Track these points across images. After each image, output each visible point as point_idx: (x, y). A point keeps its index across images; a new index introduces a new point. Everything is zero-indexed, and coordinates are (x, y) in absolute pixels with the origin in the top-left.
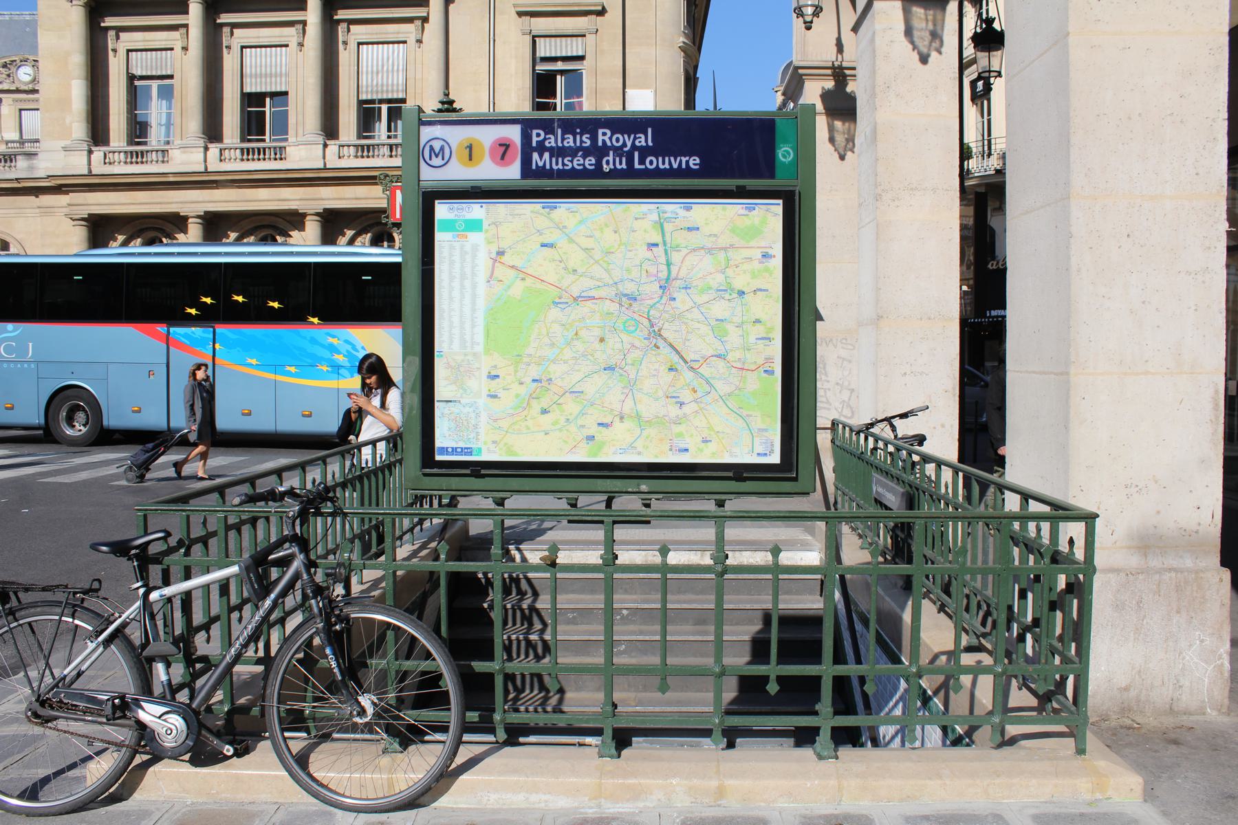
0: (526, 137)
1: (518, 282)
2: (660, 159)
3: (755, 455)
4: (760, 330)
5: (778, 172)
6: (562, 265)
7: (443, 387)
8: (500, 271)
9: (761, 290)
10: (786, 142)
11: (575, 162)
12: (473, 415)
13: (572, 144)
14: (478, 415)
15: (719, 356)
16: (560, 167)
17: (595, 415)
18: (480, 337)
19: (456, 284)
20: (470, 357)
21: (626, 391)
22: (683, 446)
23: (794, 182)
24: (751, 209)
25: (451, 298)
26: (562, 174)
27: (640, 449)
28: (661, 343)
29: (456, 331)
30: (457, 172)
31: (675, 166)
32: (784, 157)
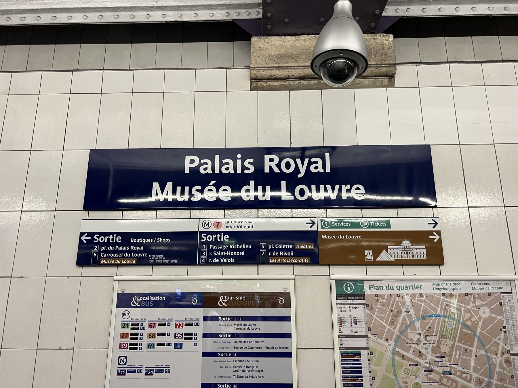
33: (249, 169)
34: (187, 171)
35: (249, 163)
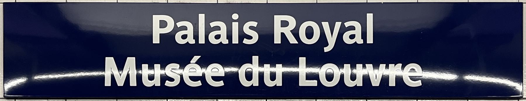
33: (250, 38)
34: (156, 40)
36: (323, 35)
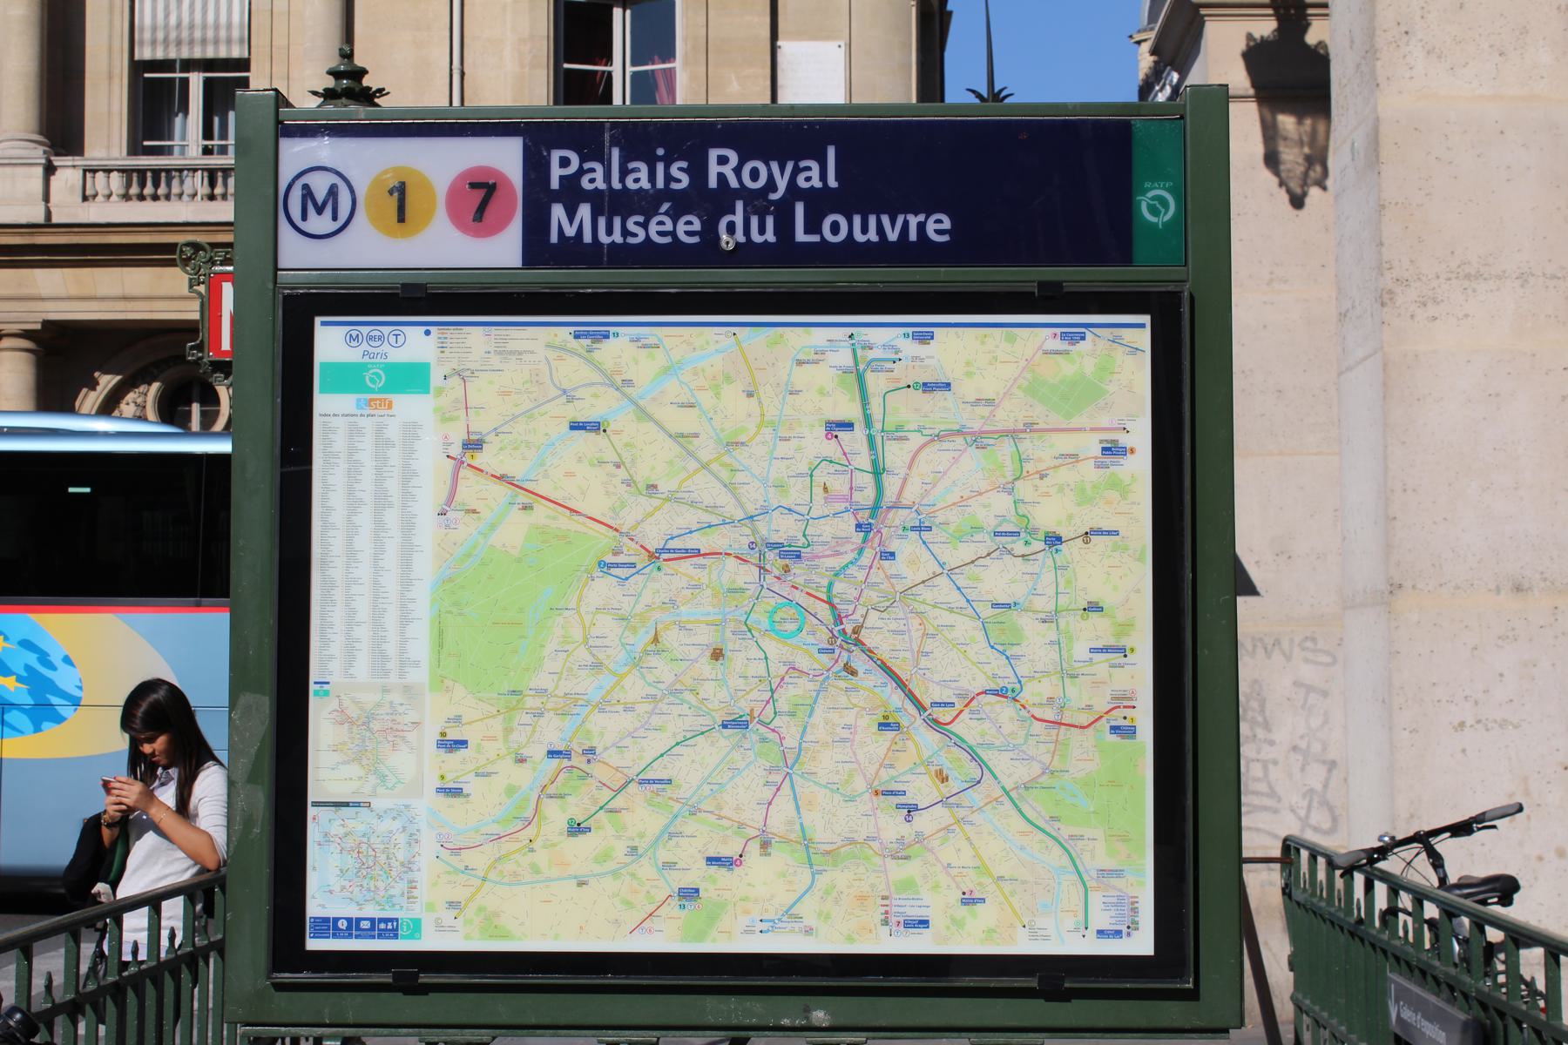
0: (535, 166)
1: (516, 514)
2: (857, 220)
3: (1091, 933)
4: (1098, 630)
5: (1141, 248)
6: (622, 473)
7: (328, 769)
8: (472, 488)
9: (1100, 532)
10: (1157, 176)
11: (653, 228)
12: (401, 839)
13: (645, 184)
14: (413, 840)
15: (996, 693)
16: (617, 237)
17: (703, 837)
18: (420, 645)
19: (364, 519)
20: (396, 697)
21: (778, 778)
22: (915, 913)
23: (1178, 272)
24: (1074, 337)
25: (351, 554)
26: (623, 255)
27: (810, 920)
28: (860, 662)
29: (363, 633)
30: (368, 249)
31: (893, 236)
32: (1154, 211)
35: (680, 169)
36: (771, 176)
